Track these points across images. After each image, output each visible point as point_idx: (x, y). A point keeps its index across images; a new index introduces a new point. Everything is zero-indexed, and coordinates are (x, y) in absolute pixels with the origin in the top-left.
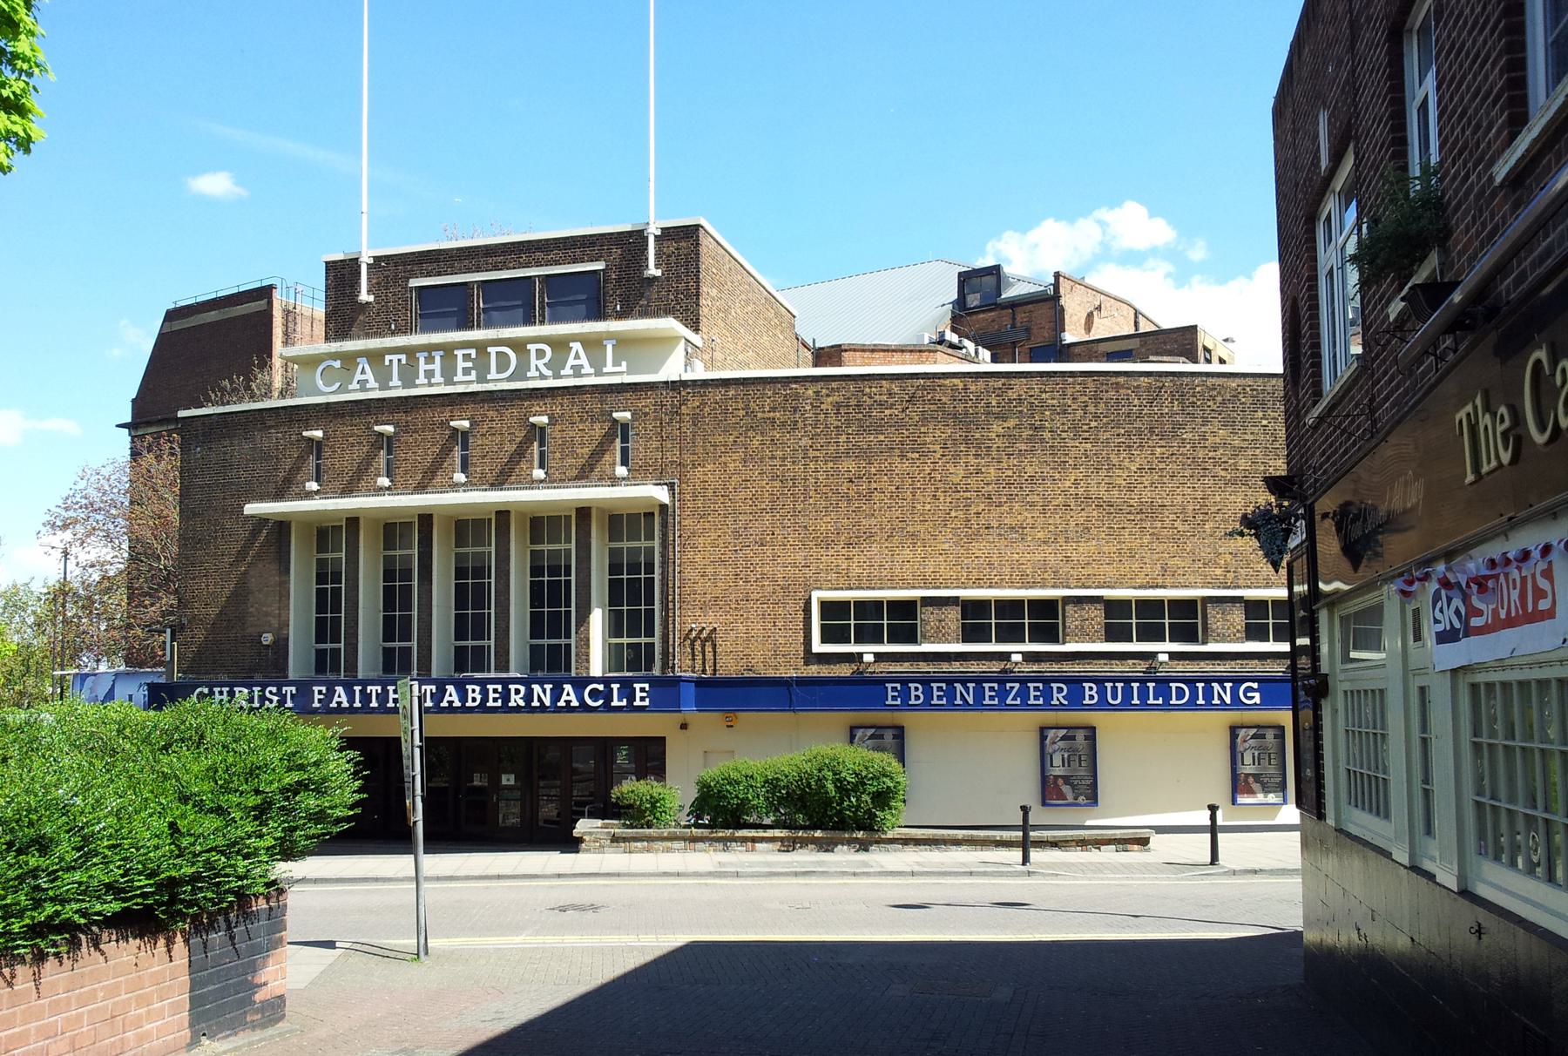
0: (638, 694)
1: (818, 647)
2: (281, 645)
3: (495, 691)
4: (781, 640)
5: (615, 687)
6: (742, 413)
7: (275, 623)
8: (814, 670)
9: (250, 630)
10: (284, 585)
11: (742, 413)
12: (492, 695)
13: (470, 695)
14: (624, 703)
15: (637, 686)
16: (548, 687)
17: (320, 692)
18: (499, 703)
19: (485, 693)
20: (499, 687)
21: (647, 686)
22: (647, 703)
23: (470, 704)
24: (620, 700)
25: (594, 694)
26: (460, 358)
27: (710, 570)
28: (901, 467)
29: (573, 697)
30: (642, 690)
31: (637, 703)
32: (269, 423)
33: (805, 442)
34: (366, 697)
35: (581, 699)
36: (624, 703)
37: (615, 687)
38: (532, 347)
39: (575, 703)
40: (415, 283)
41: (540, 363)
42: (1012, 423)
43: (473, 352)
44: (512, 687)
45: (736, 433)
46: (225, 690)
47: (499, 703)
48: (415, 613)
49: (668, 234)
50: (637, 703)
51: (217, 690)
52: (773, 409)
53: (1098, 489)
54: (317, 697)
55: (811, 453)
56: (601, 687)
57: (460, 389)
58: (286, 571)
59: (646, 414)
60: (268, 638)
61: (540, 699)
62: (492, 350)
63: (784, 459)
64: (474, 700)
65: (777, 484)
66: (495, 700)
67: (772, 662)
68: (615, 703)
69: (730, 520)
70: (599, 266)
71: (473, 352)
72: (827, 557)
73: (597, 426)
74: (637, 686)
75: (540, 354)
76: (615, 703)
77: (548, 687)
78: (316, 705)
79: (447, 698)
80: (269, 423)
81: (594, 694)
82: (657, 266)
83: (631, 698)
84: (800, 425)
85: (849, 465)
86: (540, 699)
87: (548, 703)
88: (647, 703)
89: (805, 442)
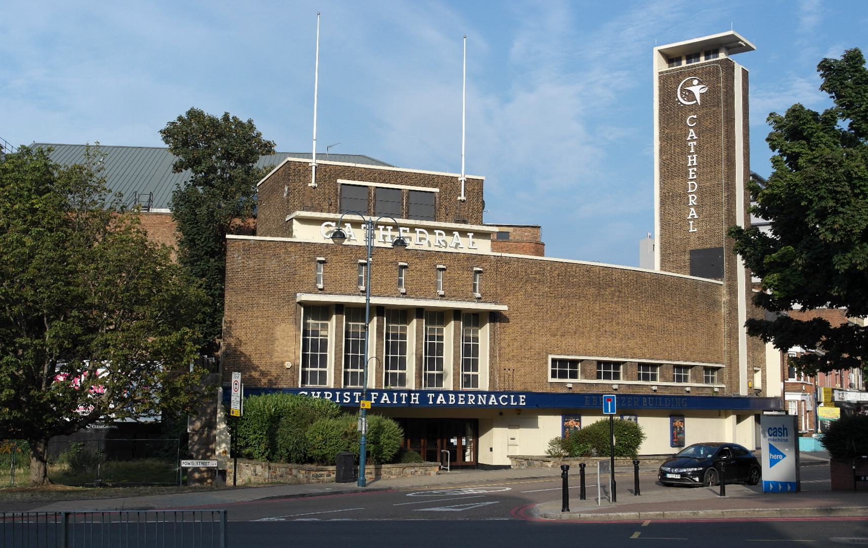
1: (550, 380)
8: (548, 390)
9: (276, 359)
19: (457, 399)
25: (504, 400)
28: (579, 304)
34: (399, 399)
35: (498, 401)
40: (340, 181)
42: (613, 289)
43: (408, 229)
46: (319, 393)
49: (468, 181)
53: (637, 319)
60: (288, 365)
67: (534, 385)
71: (408, 229)
72: (553, 341)
73: (466, 273)
81: (504, 400)
83: (518, 402)
85: (562, 301)
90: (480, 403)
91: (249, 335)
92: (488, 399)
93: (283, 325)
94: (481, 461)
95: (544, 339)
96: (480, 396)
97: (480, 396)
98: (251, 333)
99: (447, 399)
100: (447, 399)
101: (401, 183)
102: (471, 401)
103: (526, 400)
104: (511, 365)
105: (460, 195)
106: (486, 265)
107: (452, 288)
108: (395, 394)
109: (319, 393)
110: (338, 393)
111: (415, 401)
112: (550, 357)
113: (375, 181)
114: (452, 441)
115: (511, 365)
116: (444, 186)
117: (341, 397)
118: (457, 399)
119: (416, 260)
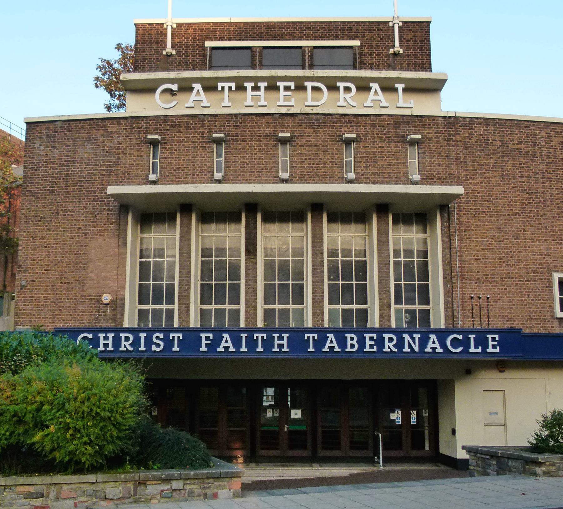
0: (491, 343)
2: (117, 305)
3: (371, 339)
4: (533, 308)
5: (472, 337)
6: (499, 143)
7: (114, 286)
10: (121, 257)
11: (499, 143)
12: (368, 343)
13: (349, 342)
14: (480, 350)
15: (490, 336)
16: (417, 336)
17: (207, 338)
18: (375, 349)
19: (362, 342)
20: (375, 336)
21: (497, 336)
22: (497, 350)
23: (349, 349)
24: (476, 347)
26: (282, 89)
27: (481, 255)
29: (437, 345)
30: (494, 339)
31: (490, 350)
32: (110, 129)
33: (542, 167)
34: (252, 343)
35: (443, 345)
36: (480, 350)
37: (472, 337)
38: (341, 85)
39: (439, 350)
41: (348, 96)
44: (386, 336)
45: (495, 158)
47: (375, 349)
48: (243, 282)
50: (490, 350)
51: (102, 335)
52: (520, 143)
54: (204, 342)
55: (547, 176)
56: (460, 337)
57: (284, 111)
58: (125, 244)
59: (430, 139)
60: (107, 298)
61: (410, 346)
62: (309, 85)
63: (529, 178)
64: (352, 346)
65: (526, 195)
66: (371, 346)
68: (472, 350)
69: (494, 219)
70: (356, 43)
73: (393, 145)
74: (490, 336)
75: (347, 89)
76: (472, 350)
77: (417, 336)
78: (204, 349)
79: (328, 344)
80: (110, 129)
81: (455, 342)
82: (401, 46)
83: (485, 346)
84: (538, 155)
86: (410, 346)
87: (417, 349)
88: (497, 350)
89: (542, 167)
90: (406, 349)
91: (52, 257)
92: (423, 342)
93: (100, 240)
94: (444, 450)
95: (543, 247)
96: (407, 337)
97: (407, 337)
98: (56, 254)
99: (342, 343)
100: (342, 343)
101: (300, 39)
102: (389, 346)
103: (500, 343)
104: (484, 290)
105: (393, 46)
106: (430, 132)
107: (372, 170)
108: (244, 336)
109: (110, 335)
110: (143, 335)
111: (281, 346)
112: (557, 276)
113: (261, 38)
114: (393, 416)
115: (484, 290)
116: (368, 36)
117: (149, 342)
118: (362, 342)
119: (308, 131)
